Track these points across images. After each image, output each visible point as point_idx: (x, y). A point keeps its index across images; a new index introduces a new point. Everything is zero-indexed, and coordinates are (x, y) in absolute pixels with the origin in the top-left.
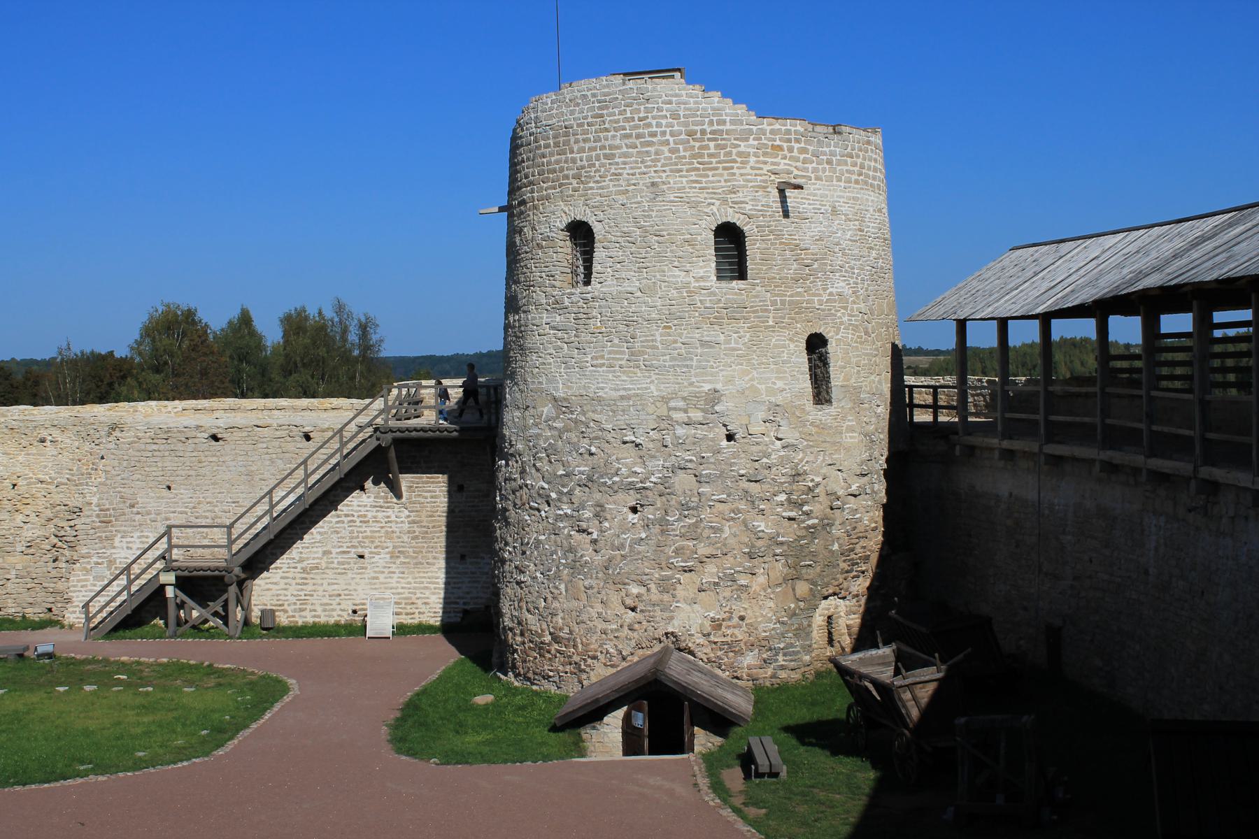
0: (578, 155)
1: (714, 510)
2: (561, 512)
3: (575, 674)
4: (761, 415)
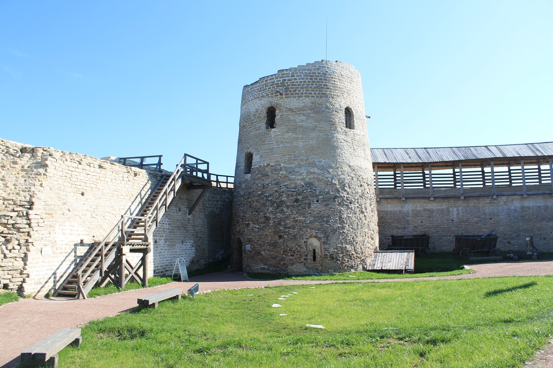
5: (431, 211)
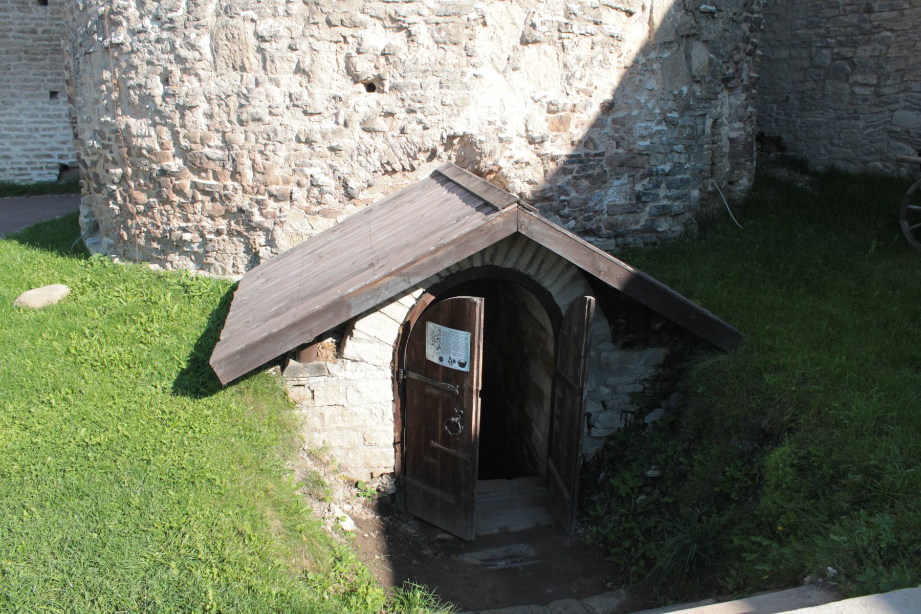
3: (239, 234)
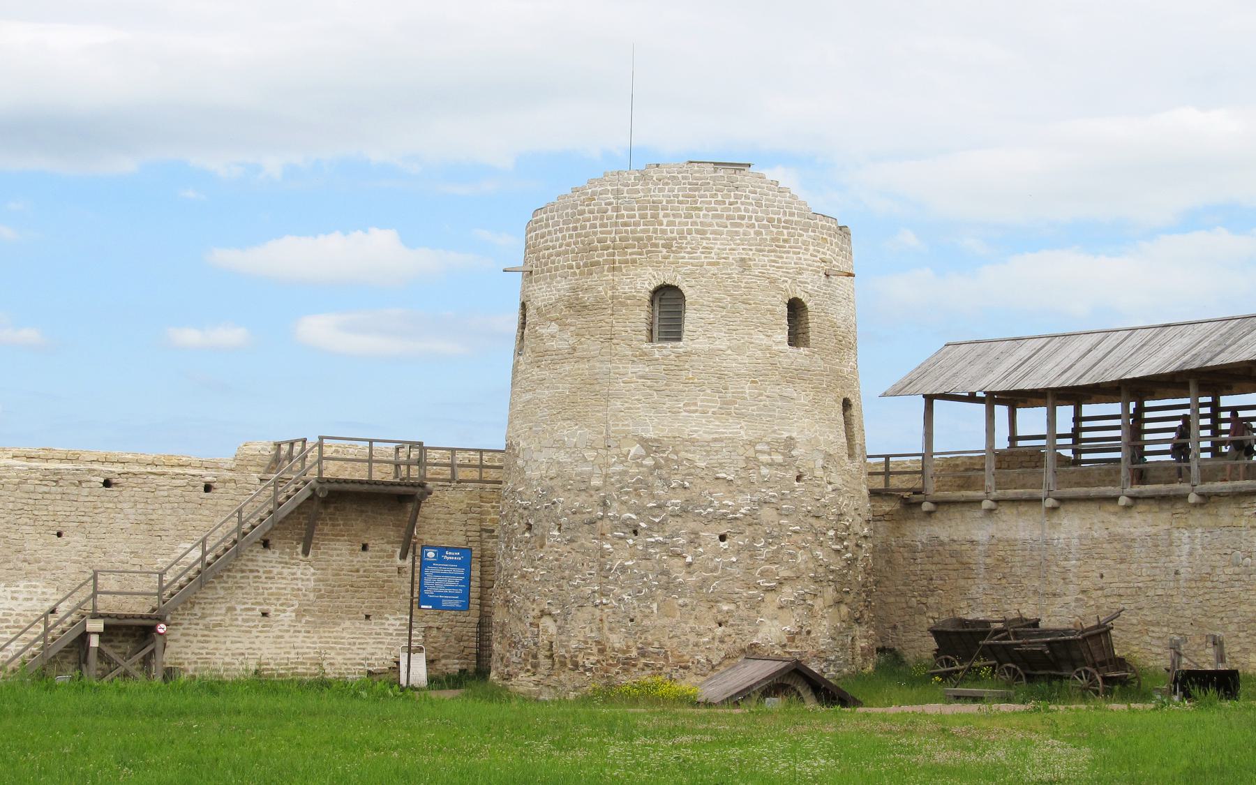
0: (669, 228)
1: (791, 539)
2: (653, 540)
4: (820, 462)
5: (1127, 542)
